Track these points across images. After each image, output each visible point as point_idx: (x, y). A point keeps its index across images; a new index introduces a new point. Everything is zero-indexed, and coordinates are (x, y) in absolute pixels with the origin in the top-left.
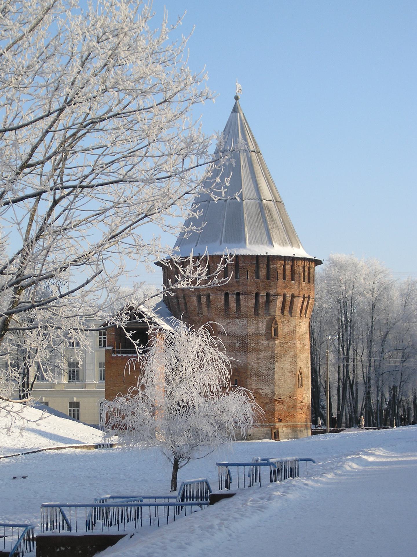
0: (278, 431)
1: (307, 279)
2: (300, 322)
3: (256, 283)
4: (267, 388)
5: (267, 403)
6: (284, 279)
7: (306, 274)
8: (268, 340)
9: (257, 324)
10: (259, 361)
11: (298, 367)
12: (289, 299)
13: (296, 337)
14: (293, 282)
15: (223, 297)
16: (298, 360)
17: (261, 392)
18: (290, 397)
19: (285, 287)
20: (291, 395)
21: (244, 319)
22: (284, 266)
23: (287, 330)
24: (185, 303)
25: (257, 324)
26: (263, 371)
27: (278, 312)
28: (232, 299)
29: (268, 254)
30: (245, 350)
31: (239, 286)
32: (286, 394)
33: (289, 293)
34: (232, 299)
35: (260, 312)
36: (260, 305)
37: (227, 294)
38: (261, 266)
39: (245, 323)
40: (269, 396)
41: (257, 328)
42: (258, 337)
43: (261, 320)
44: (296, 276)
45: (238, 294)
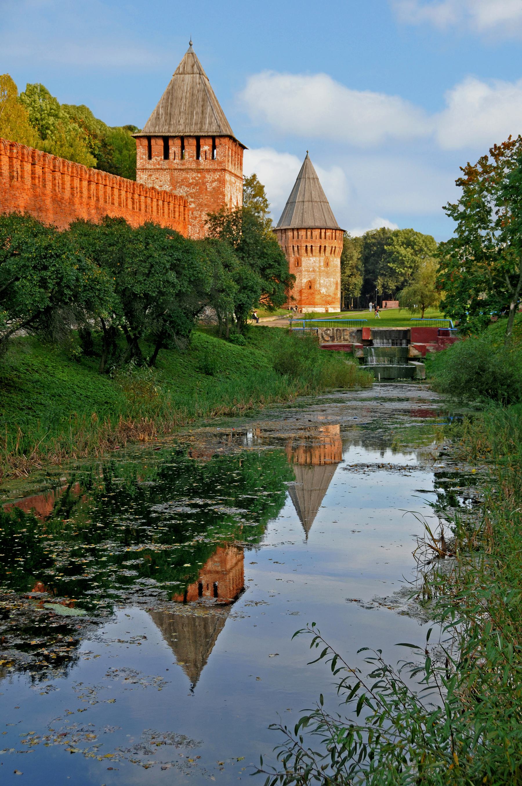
26: (322, 282)
28: (309, 248)
33: (334, 246)
34: (309, 248)
37: (306, 246)
41: (320, 262)
42: (320, 266)
45: (312, 246)
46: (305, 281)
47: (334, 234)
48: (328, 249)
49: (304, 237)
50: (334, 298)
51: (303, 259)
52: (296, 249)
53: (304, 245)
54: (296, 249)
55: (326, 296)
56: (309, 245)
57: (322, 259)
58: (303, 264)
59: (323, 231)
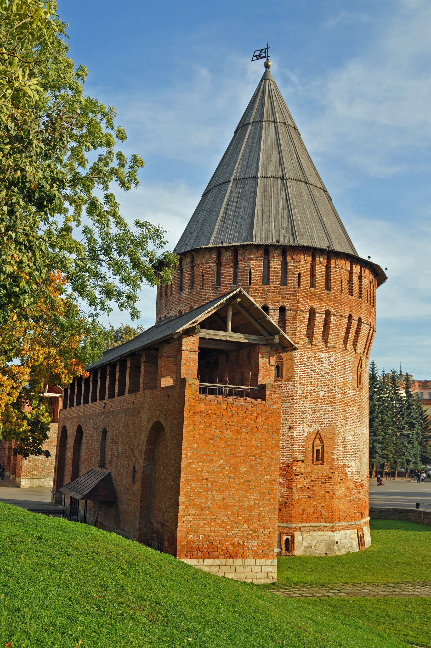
9: (344, 363)
15: (307, 315)
17: (348, 470)
21: (331, 353)
25: (344, 363)
28: (320, 320)
29: (370, 260)
30: (331, 402)
31: (331, 300)
34: (320, 320)
37: (312, 312)
39: (332, 359)
40: (355, 478)
46: (302, 431)
49: (306, 279)
53: (305, 306)
56: (320, 309)
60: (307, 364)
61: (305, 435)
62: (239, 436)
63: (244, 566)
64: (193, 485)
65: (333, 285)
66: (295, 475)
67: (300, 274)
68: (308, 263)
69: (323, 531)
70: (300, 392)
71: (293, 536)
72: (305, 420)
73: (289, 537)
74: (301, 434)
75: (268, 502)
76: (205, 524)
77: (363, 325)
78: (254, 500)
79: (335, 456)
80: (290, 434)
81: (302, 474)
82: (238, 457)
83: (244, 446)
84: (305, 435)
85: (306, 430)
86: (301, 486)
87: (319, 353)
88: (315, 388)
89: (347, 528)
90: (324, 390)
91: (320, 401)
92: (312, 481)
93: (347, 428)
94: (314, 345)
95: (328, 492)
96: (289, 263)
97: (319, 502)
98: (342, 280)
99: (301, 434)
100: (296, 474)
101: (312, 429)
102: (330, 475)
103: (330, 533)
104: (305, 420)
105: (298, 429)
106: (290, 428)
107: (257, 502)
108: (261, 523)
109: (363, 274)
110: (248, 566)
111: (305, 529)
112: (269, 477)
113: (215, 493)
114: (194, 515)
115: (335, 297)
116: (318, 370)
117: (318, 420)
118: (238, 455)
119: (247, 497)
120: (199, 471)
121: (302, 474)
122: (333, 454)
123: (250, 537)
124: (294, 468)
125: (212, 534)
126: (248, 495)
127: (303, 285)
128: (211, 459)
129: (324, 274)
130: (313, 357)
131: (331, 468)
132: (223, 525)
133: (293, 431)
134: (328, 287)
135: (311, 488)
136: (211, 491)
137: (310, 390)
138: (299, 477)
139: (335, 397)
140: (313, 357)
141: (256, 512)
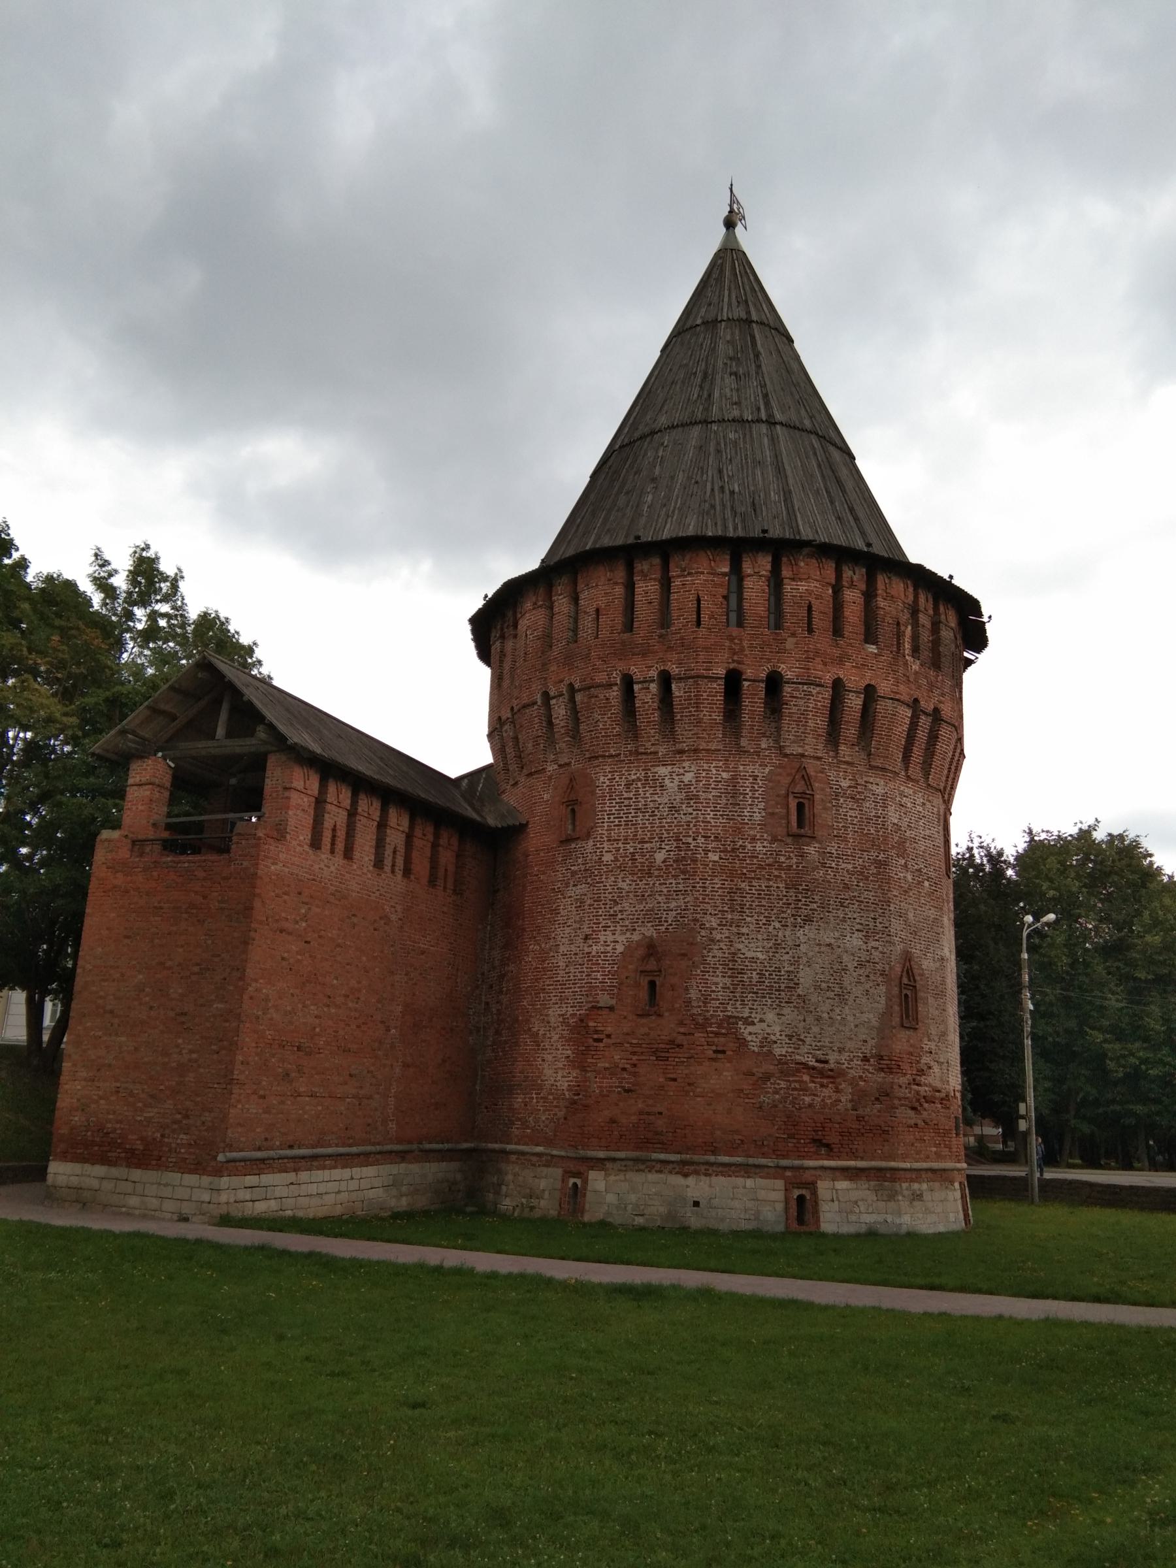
0: (814, 1193)
1: (926, 654)
2: (902, 795)
3: (731, 638)
4: (770, 1016)
5: (767, 1077)
6: (837, 631)
7: (925, 636)
8: (774, 839)
10: (736, 916)
11: (899, 948)
12: (854, 702)
13: (885, 838)
14: (872, 649)
15: (615, 693)
16: (896, 925)
17: (745, 1031)
18: (865, 1059)
19: (840, 661)
20: (867, 1050)
21: (686, 764)
22: (837, 590)
23: (848, 809)
24: (516, 739)
26: (753, 950)
27: (813, 746)
28: (647, 697)
30: (684, 872)
31: (670, 648)
32: (850, 1045)
33: (854, 680)
34: (647, 697)
35: (744, 742)
36: (746, 717)
37: (628, 682)
38: (748, 583)
39: (688, 777)
40: (778, 1051)
43: (750, 768)
44: (885, 630)
46: (615, 941)
47: (853, 597)
48: (807, 706)
49: (614, 618)
50: (884, 1094)
51: (603, 780)
52: (560, 710)
54: (560, 710)
55: (789, 1069)
56: (645, 671)
57: (757, 771)
58: (607, 818)
59: (757, 568)
60: (626, 795)
61: (618, 952)
62: (174, 928)
63: (159, 1184)
64: (89, 1024)
65: (675, 614)
66: (596, 1040)
67: (597, 610)
68: (616, 583)
69: (660, 1172)
70: (607, 858)
71: (585, 1182)
72: (620, 916)
73: (579, 1182)
74: (609, 949)
75: (215, 1056)
76: (101, 1098)
77: (787, 689)
78: (191, 1052)
79: (693, 994)
80: (587, 950)
81: (609, 1036)
82: (169, 968)
83: (182, 946)
84: (618, 952)
85: (621, 938)
86: (607, 1065)
87: (657, 769)
88: (646, 846)
89: (747, 1170)
90: (667, 848)
91: (656, 873)
92: (634, 1053)
93: (744, 930)
94: (642, 753)
95: (675, 1080)
96: (582, 596)
97: (650, 1102)
98: (699, 600)
99: (609, 949)
100: (596, 1036)
101: (636, 937)
102: (680, 1039)
103: (679, 1180)
104: (620, 916)
105: (602, 938)
106: (586, 938)
107: (194, 1056)
108: (199, 1099)
109: (786, 572)
110: (166, 1185)
111: (618, 1165)
112: (220, 1006)
113: (123, 1039)
114: (85, 1080)
115: (682, 638)
116: (652, 805)
117: (652, 916)
118: (169, 963)
119: (177, 1046)
120: (101, 997)
121: (609, 1036)
122: (687, 989)
123: (175, 1126)
124: (591, 1024)
125: (111, 1116)
126: (180, 1041)
127: (604, 633)
128: (123, 975)
129: (655, 597)
130: (640, 780)
131: (681, 1023)
132: (131, 1099)
133: (590, 942)
134: (664, 621)
135: (633, 1070)
136: (117, 1035)
137: (632, 850)
138: (601, 1045)
139: (695, 861)
140: (640, 780)
141: (191, 1077)
